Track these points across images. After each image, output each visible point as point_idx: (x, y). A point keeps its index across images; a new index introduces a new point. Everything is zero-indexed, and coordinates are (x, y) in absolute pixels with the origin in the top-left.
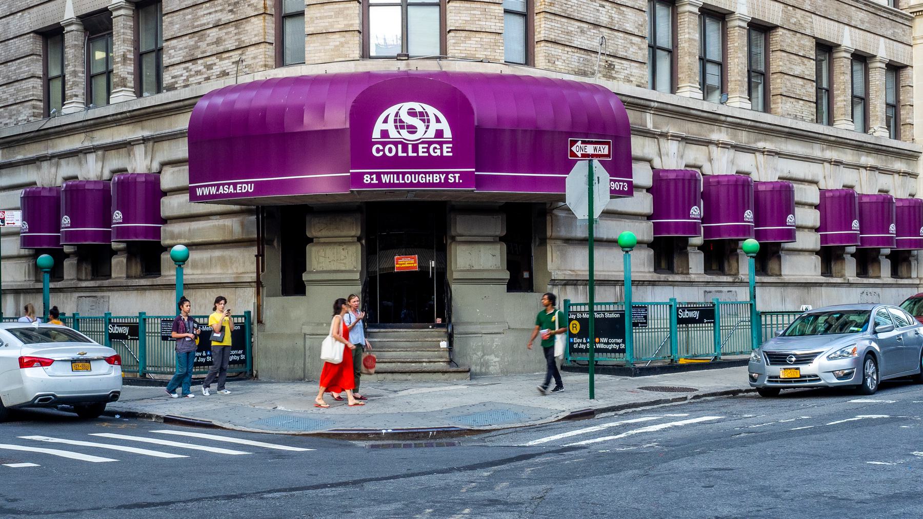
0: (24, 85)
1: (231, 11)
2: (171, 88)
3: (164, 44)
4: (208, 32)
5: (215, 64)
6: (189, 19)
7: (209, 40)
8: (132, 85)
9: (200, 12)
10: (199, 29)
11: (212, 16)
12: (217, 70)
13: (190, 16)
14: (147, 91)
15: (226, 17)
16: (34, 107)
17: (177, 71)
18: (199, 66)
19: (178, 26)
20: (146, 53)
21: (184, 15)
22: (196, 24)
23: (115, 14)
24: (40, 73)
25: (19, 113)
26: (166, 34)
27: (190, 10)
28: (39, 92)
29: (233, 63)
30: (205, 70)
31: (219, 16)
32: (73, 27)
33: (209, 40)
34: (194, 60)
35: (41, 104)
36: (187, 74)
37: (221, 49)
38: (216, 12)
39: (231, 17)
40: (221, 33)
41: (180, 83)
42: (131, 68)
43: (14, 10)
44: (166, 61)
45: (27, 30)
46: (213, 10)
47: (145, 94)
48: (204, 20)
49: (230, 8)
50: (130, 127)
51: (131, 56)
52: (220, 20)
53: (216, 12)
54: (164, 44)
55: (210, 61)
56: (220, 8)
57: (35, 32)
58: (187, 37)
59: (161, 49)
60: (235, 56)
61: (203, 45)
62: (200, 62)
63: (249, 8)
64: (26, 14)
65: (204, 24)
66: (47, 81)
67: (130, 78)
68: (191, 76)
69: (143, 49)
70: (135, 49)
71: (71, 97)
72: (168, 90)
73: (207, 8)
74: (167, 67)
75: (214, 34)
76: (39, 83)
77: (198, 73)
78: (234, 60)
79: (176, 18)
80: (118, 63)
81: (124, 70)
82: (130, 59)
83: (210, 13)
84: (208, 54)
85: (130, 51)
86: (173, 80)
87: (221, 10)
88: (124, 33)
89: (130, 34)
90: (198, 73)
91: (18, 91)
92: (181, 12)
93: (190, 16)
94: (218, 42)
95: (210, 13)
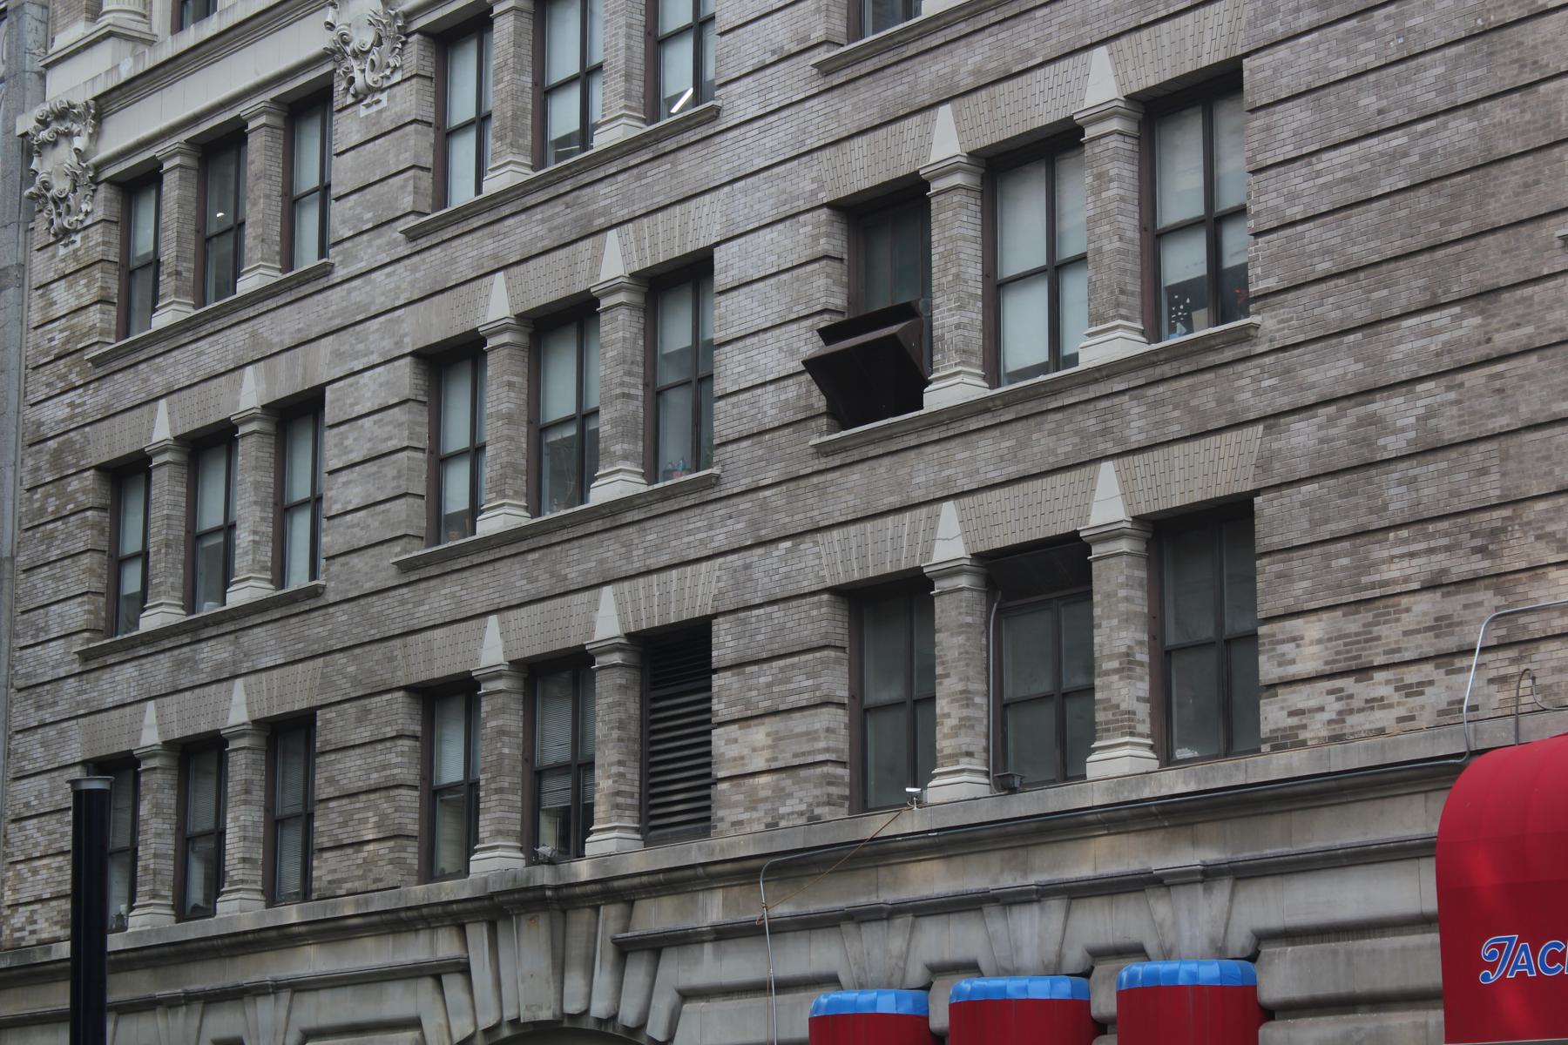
0: (798, 723)
1: (1477, 550)
2: (1286, 741)
3: (1262, 630)
4: (1405, 601)
5: (1431, 683)
6: (1344, 569)
7: (1408, 621)
8: (1145, 728)
9: (1379, 552)
10: (1377, 593)
11: (1415, 562)
12: (1436, 697)
13: (1345, 561)
14: (1185, 743)
15: (1462, 565)
16: (831, 781)
17: (1301, 698)
18: (1380, 685)
19: (1305, 584)
20: (1181, 649)
21: (1327, 558)
22: (1364, 580)
23: (1097, 550)
24: (842, 693)
25: (781, 795)
26: (1266, 607)
27: (1346, 544)
28: (841, 743)
29: (1491, 681)
30: (1396, 697)
31: (1439, 561)
32: (963, 581)
33: (1408, 621)
34: (1363, 672)
35: (844, 772)
36: (1339, 706)
37: (1450, 643)
38: (1431, 551)
39: (1481, 565)
40: (1454, 604)
41: (1317, 728)
42: (1143, 688)
43: (766, 533)
44: (1268, 670)
45: (807, 585)
46: (1422, 546)
47: (1182, 753)
48: (1393, 572)
49: (1478, 542)
50: (1156, 837)
51: (1142, 656)
52: (1445, 571)
53: (1431, 551)
54: (1262, 630)
55: (1412, 675)
56: (1444, 541)
57: (833, 591)
58: (1339, 613)
59: (1253, 637)
60: (1500, 663)
61: (1390, 633)
62: (1379, 676)
63: (1541, 545)
64: (807, 545)
65: (1394, 582)
66: (862, 713)
67: (1143, 710)
68: (1351, 712)
69: (1172, 639)
70: (1153, 637)
71: (954, 757)
72: (1276, 748)
73: (1405, 541)
74: (1272, 687)
75: (1424, 607)
76: (836, 719)
77: (1373, 703)
78: (1493, 674)
79: (1297, 564)
80: (1107, 673)
81: (1124, 692)
82: (1141, 664)
83: (1412, 555)
84: (1407, 656)
85: (1140, 643)
86: (1294, 721)
87: (1448, 548)
88: (1127, 599)
89: (1140, 603)
90: (1373, 703)
91: (777, 739)
92: (1317, 551)
93: (1345, 561)
94: (1441, 624)
95: (1412, 555)
